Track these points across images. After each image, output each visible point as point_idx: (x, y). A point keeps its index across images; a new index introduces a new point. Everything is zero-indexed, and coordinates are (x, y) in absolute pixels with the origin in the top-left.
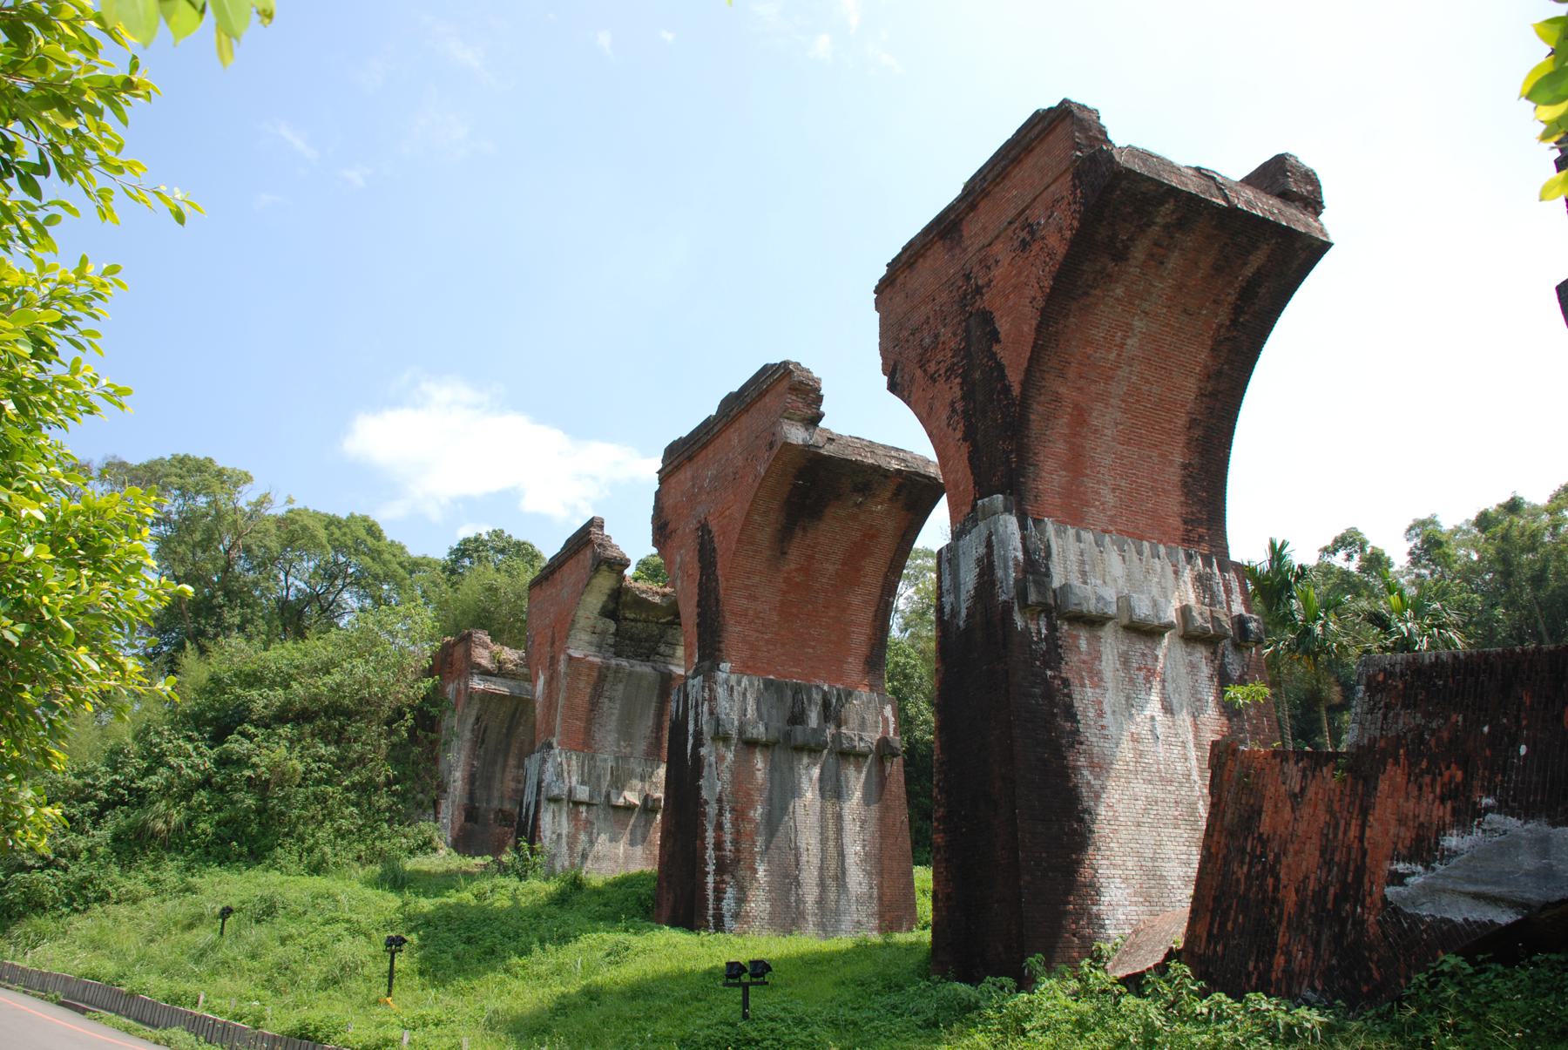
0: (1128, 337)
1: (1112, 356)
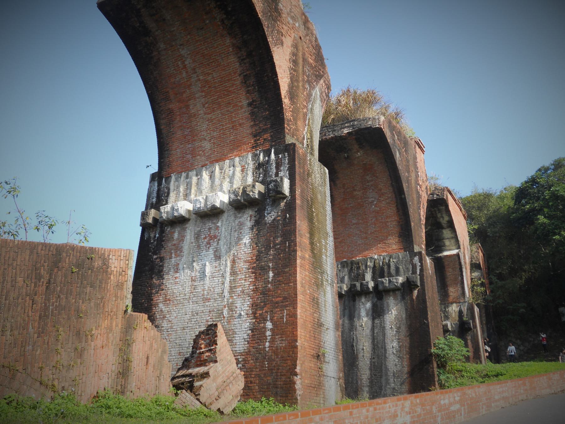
0: (185, 61)
1: (184, 75)
